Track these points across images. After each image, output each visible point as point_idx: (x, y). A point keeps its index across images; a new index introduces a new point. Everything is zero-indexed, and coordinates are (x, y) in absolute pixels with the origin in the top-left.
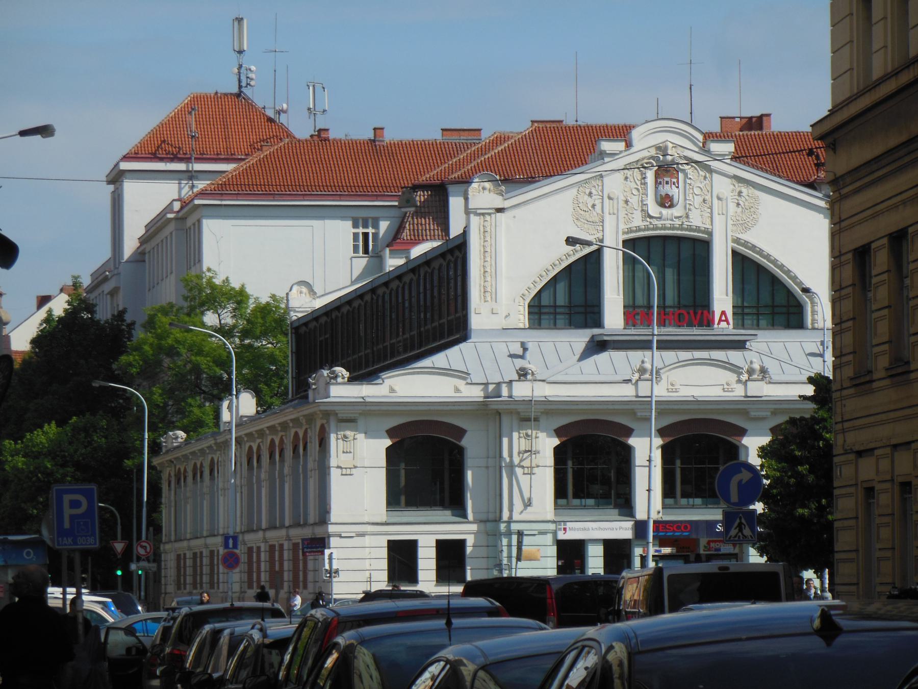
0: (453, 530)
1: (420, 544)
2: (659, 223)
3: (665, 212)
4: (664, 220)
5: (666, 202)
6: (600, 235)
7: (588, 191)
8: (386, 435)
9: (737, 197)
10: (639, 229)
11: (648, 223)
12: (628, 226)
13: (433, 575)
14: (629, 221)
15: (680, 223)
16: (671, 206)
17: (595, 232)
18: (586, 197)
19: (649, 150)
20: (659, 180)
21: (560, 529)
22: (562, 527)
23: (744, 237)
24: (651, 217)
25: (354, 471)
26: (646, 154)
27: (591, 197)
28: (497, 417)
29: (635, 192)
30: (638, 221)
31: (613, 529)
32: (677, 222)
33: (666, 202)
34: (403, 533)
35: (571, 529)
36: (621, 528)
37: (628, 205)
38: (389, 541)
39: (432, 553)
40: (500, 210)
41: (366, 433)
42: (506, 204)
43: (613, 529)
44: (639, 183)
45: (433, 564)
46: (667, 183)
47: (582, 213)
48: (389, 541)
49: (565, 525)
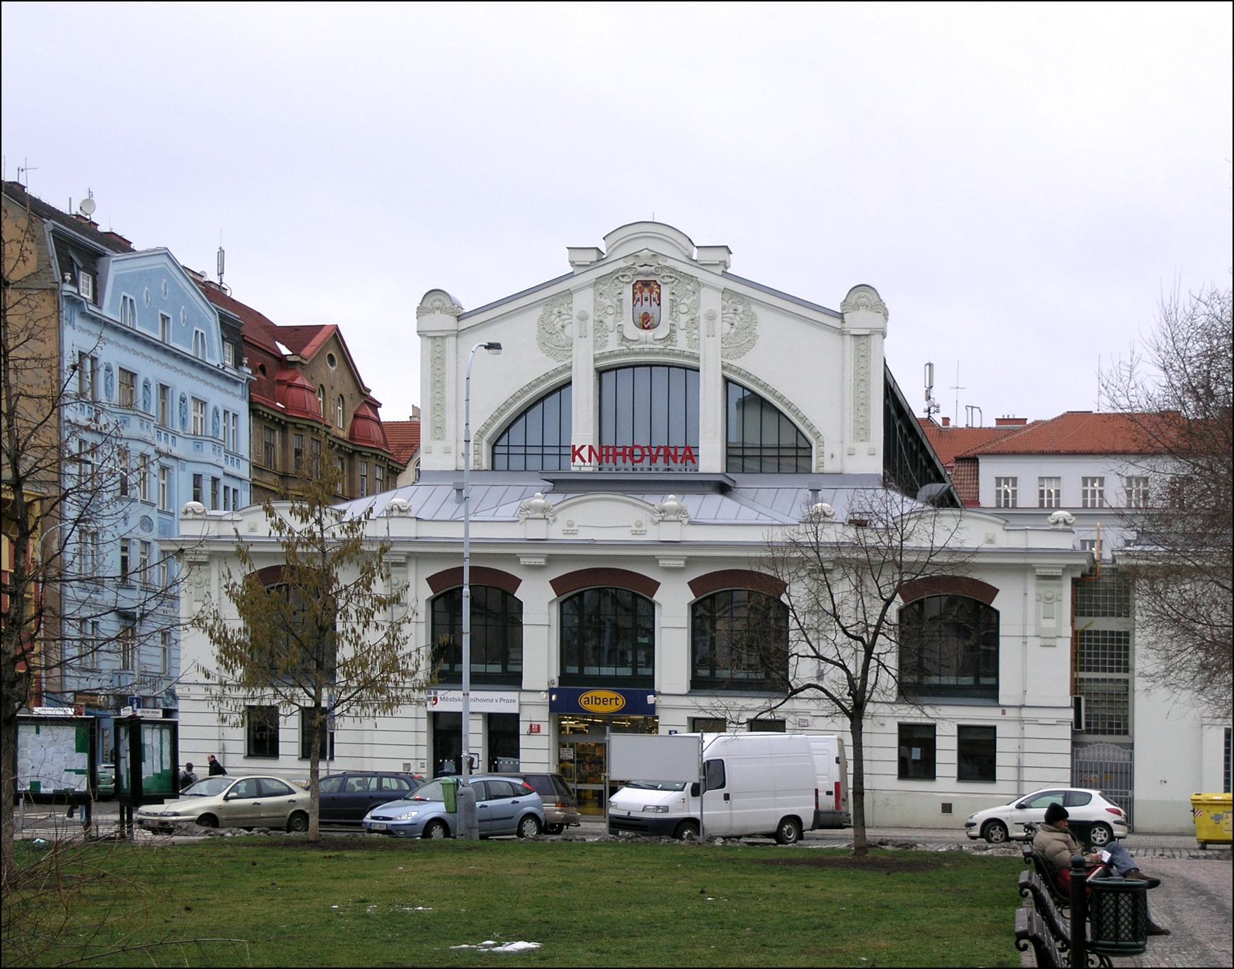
2: (636, 347)
4: (641, 343)
6: (567, 362)
7: (555, 310)
10: (612, 355)
11: (624, 348)
12: (601, 351)
14: (604, 345)
15: (662, 347)
23: (737, 363)
26: (622, 264)
30: (613, 345)
47: (548, 335)
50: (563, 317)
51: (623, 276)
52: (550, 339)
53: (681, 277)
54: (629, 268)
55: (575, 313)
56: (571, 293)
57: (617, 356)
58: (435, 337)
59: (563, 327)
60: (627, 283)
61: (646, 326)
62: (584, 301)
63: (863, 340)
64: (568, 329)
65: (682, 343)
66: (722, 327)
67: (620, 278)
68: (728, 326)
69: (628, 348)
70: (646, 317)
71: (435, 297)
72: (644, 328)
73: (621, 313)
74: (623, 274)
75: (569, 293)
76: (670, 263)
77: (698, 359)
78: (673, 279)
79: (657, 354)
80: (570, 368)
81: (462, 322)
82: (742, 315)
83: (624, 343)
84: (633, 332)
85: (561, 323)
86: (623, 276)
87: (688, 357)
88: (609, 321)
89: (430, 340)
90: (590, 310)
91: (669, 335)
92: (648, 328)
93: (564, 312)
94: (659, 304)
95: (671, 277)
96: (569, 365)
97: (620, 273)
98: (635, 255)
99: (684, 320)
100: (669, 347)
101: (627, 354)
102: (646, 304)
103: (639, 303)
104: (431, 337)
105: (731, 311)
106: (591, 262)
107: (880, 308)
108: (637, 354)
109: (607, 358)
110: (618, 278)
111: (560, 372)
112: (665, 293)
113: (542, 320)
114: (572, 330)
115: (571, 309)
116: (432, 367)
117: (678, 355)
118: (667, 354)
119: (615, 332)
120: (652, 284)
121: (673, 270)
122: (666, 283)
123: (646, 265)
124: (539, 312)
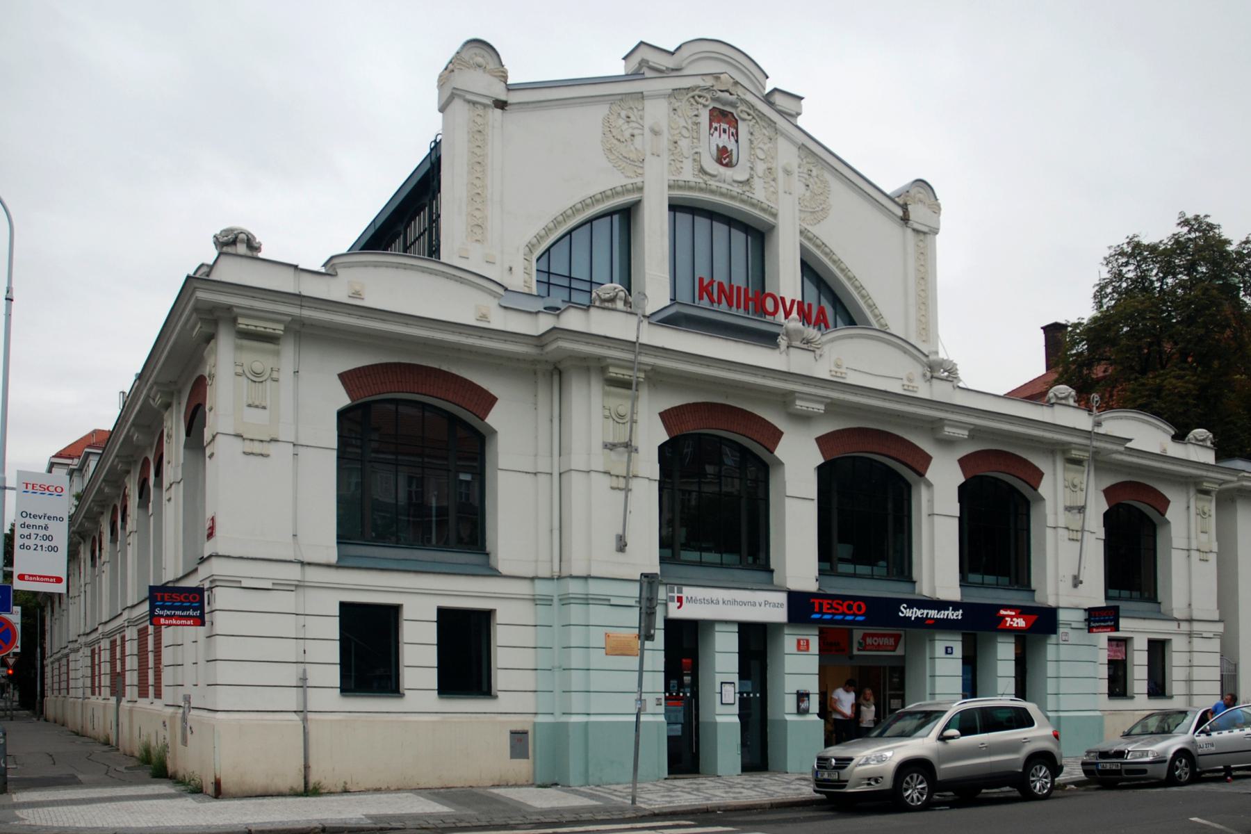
1: (406, 614)
2: (713, 184)
3: (722, 169)
5: (724, 157)
6: (638, 180)
7: (623, 114)
9: (807, 176)
10: (687, 186)
11: (701, 181)
12: (676, 178)
15: (740, 191)
16: (729, 165)
17: (633, 175)
18: (621, 122)
19: (704, 78)
20: (715, 125)
21: (672, 599)
22: (676, 595)
23: (814, 230)
24: (706, 173)
25: (271, 449)
26: (698, 82)
27: (628, 122)
28: (556, 378)
29: (685, 132)
30: (688, 174)
31: (754, 604)
32: (736, 189)
33: (724, 157)
35: (690, 600)
36: (766, 603)
37: (676, 147)
38: (343, 605)
39: (431, 633)
43: (754, 604)
44: (689, 122)
46: (725, 131)
47: (615, 142)
48: (343, 605)
49: (680, 591)
51: (700, 97)
53: (760, 117)
54: (707, 89)
55: (648, 122)
56: (643, 98)
57: (691, 188)
58: (474, 103)
60: (705, 106)
61: (724, 162)
62: (656, 112)
63: (922, 237)
64: (638, 139)
65: (759, 193)
66: (798, 188)
67: (696, 97)
68: (804, 187)
71: (478, 51)
72: (721, 164)
73: (699, 140)
74: (700, 93)
75: (641, 96)
76: (749, 97)
77: (775, 215)
78: (750, 117)
79: (732, 198)
80: (641, 189)
81: (512, 93)
82: (816, 179)
83: (701, 175)
85: (630, 131)
86: (700, 97)
87: (763, 210)
88: (684, 144)
89: (466, 106)
90: (664, 125)
91: (748, 180)
92: (726, 165)
93: (633, 118)
94: (737, 141)
95: (749, 115)
96: (640, 185)
97: (697, 92)
98: (716, 77)
99: (760, 168)
100: (747, 194)
101: (701, 190)
102: (725, 136)
103: (717, 134)
104: (469, 102)
105: (805, 171)
106: (667, 68)
107: (936, 208)
108: (712, 192)
109: (680, 188)
110: (693, 97)
112: (743, 128)
113: (607, 120)
114: (644, 142)
115: (642, 118)
116: (469, 141)
117: (753, 205)
118: (743, 201)
119: (690, 160)
120: (730, 116)
121: (752, 107)
122: (744, 120)
123: (727, 91)
124: (602, 110)
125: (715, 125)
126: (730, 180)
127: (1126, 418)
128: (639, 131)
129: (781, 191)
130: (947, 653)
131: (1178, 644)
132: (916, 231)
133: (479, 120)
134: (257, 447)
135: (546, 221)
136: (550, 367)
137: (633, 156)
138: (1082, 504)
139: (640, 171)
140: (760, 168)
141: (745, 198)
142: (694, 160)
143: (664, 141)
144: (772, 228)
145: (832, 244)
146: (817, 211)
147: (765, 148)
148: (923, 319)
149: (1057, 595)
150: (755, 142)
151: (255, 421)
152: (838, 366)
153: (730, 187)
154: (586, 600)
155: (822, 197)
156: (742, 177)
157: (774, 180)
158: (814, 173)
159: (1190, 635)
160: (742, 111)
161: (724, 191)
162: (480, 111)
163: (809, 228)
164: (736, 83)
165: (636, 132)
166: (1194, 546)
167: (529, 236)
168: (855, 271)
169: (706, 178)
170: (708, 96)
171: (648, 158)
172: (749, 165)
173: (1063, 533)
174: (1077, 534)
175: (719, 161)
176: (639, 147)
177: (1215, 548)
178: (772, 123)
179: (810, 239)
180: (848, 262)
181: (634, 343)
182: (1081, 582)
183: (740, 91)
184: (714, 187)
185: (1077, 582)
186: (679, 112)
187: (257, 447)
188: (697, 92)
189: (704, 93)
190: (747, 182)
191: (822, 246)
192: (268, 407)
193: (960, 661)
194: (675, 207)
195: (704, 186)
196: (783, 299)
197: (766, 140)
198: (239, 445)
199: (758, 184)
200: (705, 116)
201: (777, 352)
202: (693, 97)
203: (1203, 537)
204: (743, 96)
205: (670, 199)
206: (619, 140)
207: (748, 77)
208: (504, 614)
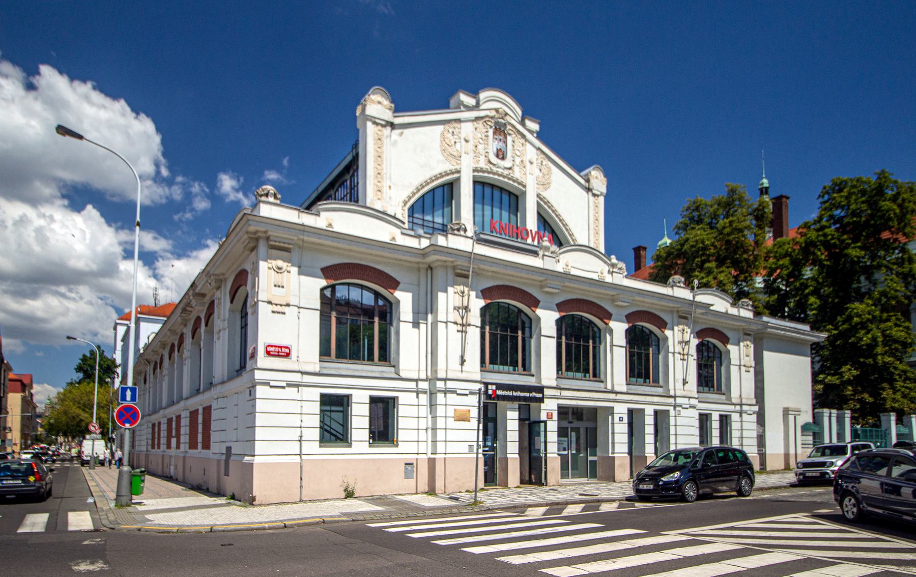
0: (384, 387)
2: (495, 169)
4: (498, 167)
6: (458, 167)
7: (451, 131)
8: (321, 274)
10: (482, 171)
11: (488, 168)
13: (365, 434)
16: (503, 158)
17: (455, 164)
18: (449, 135)
23: (544, 194)
29: (481, 141)
30: (483, 164)
32: (506, 172)
34: (336, 385)
39: (365, 410)
40: (392, 126)
41: (299, 267)
42: (397, 121)
44: (483, 135)
45: (365, 422)
47: (447, 146)
50: (455, 137)
51: (488, 121)
52: (445, 148)
54: (492, 118)
55: (463, 136)
57: (483, 172)
59: (455, 143)
63: (596, 198)
64: (458, 145)
65: (517, 174)
66: (537, 172)
68: (539, 171)
69: (491, 168)
70: (499, 150)
73: (488, 144)
76: (513, 122)
77: (525, 186)
79: (504, 177)
80: (459, 172)
83: (489, 164)
84: (494, 160)
85: (454, 140)
88: (480, 147)
93: (455, 133)
94: (506, 146)
98: (497, 110)
99: (518, 160)
100: (511, 175)
101: (489, 173)
110: (485, 122)
111: (453, 173)
112: (509, 139)
113: (442, 134)
114: (461, 146)
115: (459, 133)
116: (375, 144)
117: (514, 181)
118: (509, 179)
119: (484, 156)
124: (440, 128)
125: (496, 137)
126: (502, 167)
127: (708, 294)
128: (459, 140)
129: (528, 173)
130: (620, 420)
131: (735, 417)
132: (594, 195)
133: (379, 133)
134: (278, 309)
135: (412, 189)
136: (427, 266)
137: (455, 154)
138: (688, 340)
139: (459, 162)
140: (518, 160)
141: (510, 177)
142: (486, 156)
143: (470, 146)
144: (524, 193)
145: (553, 202)
146: (545, 185)
147: (520, 149)
148: (597, 242)
149: (675, 390)
150: (515, 147)
151: (278, 295)
152: (567, 266)
153: (503, 171)
154: (445, 392)
155: (548, 176)
156: (508, 166)
157: (524, 167)
158: (544, 163)
159: (741, 413)
160: (509, 129)
161: (500, 173)
162: (380, 127)
163: (541, 193)
164: (506, 114)
165: (457, 140)
166: (742, 364)
167: (404, 196)
168: (564, 216)
169: (491, 166)
170: (493, 121)
171: (463, 155)
172: (512, 159)
173: (677, 356)
174: (684, 356)
175: (497, 156)
176: (459, 149)
177: (753, 364)
178: (524, 136)
179: (541, 199)
180: (560, 211)
181: (471, 253)
182: (687, 382)
183: (508, 118)
184: (495, 171)
185: (685, 382)
186: (478, 130)
187: (278, 309)
188: (487, 119)
189: (490, 120)
190: (510, 169)
191: (547, 203)
192: (285, 286)
193: (626, 425)
194: (476, 182)
195: (489, 170)
196: (531, 231)
197: (521, 145)
198: (271, 308)
199: (516, 169)
200: (491, 131)
201: (537, 259)
202: (485, 122)
203: (747, 359)
204: (509, 121)
205: (474, 177)
206: (448, 145)
207: (513, 112)
208: (403, 398)
